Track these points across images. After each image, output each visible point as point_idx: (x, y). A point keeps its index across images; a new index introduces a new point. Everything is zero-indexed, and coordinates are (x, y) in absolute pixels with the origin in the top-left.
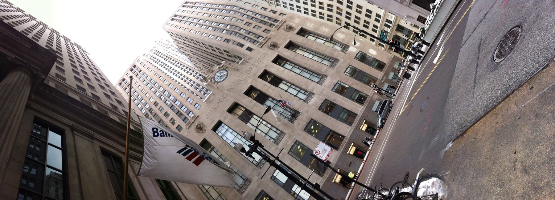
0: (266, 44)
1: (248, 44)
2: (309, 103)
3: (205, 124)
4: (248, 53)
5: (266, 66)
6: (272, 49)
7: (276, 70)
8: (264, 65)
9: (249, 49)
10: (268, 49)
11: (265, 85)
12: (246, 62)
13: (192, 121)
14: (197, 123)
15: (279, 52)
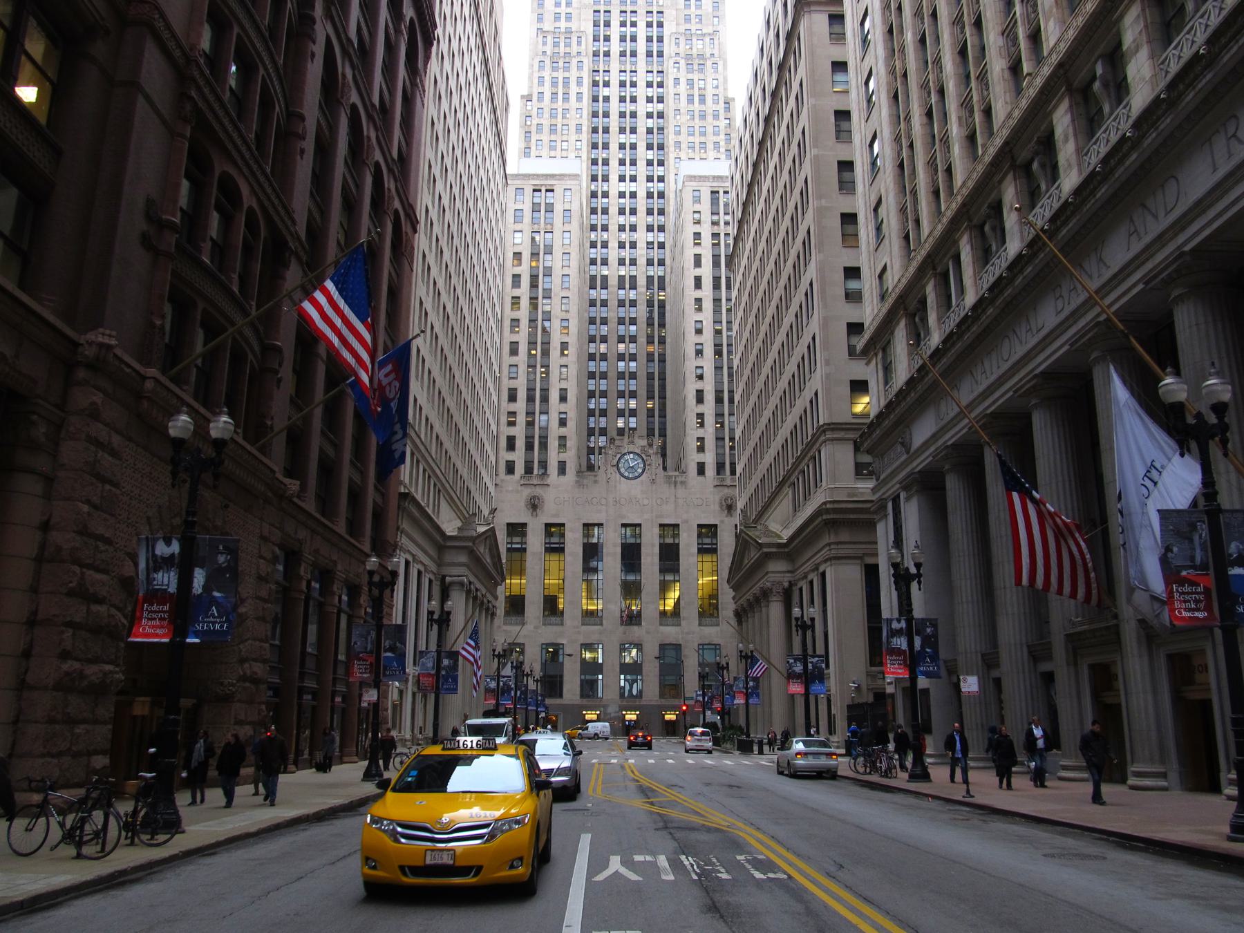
0: (726, 490)
1: (709, 458)
2: (662, 628)
3: (546, 508)
4: (693, 469)
5: (686, 522)
6: (721, 506)
7: (688, 542)
8: (685, 516)
9: (701, 469)
10: (717, 498)
11: (653, 545)
12: (675, 483)
13: (535, 482)
14: (539, 491)
15: (722, 522)
